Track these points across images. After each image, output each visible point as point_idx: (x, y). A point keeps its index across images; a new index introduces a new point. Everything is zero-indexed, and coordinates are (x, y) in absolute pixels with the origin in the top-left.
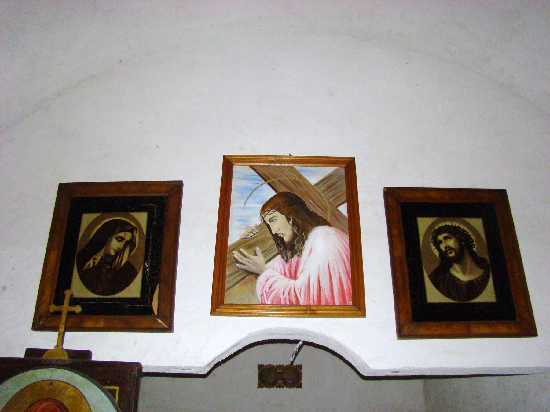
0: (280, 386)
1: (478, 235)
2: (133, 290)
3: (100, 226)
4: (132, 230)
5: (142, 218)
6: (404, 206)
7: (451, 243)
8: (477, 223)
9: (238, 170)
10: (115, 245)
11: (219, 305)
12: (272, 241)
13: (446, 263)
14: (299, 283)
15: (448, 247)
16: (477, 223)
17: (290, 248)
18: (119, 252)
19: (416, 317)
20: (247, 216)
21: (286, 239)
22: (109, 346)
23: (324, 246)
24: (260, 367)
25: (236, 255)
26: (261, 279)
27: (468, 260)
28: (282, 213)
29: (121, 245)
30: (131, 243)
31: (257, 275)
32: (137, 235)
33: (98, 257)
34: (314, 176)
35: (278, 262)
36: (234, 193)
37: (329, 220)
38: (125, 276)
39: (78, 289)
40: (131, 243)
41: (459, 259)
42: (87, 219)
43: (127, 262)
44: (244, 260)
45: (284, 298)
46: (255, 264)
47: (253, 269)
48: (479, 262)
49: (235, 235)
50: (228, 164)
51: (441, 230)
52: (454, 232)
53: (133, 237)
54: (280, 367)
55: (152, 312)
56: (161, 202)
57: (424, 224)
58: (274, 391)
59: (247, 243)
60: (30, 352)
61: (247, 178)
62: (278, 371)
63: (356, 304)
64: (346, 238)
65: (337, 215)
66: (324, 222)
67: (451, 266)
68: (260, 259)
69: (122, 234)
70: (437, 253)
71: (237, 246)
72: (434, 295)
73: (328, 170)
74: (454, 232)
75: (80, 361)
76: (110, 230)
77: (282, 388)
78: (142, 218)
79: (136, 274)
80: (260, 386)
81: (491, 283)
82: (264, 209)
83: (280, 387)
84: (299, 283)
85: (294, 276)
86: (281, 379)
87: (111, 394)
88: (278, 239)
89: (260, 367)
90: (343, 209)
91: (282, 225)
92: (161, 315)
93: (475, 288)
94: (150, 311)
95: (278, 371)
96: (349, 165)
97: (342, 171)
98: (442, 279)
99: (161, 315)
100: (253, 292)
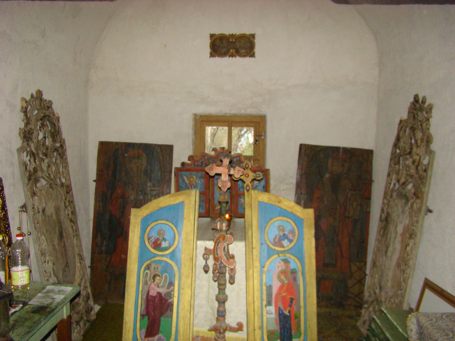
0: (232, 56)
24: (212, 36)
54: (232, 36)
58: (226, 60)
62: (231, 40)
77: (234, 58)
80: (212, 55)
83: (232, 57)
86: (234, 48)
89: (212, 36)
95: (231, 40)
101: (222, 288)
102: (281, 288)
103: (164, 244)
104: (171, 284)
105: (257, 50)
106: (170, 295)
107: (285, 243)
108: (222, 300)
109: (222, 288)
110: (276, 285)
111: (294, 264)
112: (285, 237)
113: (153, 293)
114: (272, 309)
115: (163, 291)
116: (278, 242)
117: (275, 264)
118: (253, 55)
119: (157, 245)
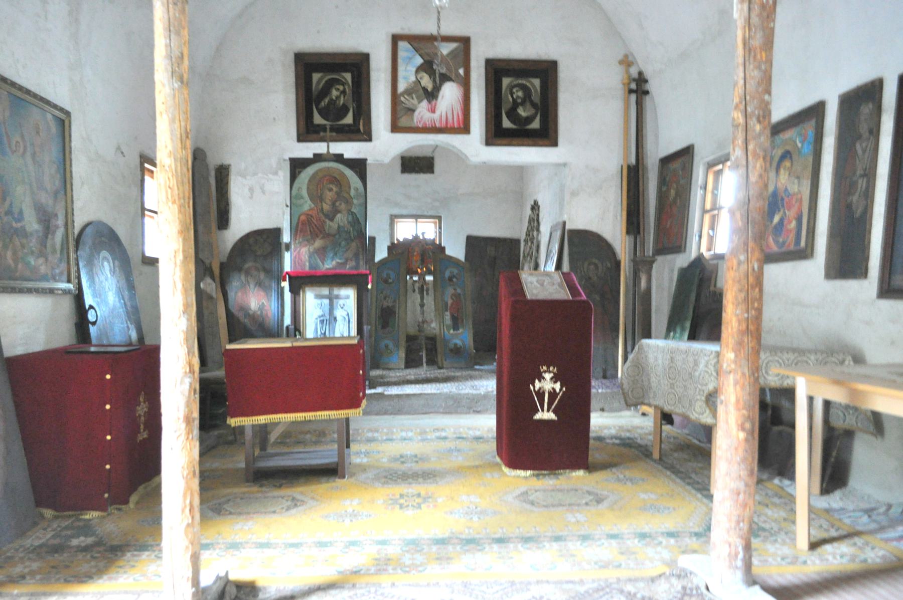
1: (536, 91)
2: (349, 119)
3: (324, 82)
4: (343, 84)
5: (348, 76)
6: (497, 70)
7: (520, 94)
8: (537, 82)
9: (403, 45)
10: (335, 93)
11: (396, 128)
12: (421, 91)
13: (515, 106)
14: (436, 116)
15: (518, 97)
16: (537, 82)
17: (431, 95)
18: (338, 98)
19: (496, 135)
20: (408, 75)
21: (429, 90)
22: (350, 149)
23: (450, 93)
25: (402, 99)
26: (416, 113)
27: (528, 105)
28: (426, 72)
29: (338, 93)
30: (344, 92)
31: (413, 111)
32: (346, 87)
33: (327, 100)
34: (446, 49)
35: (425, 103)
36: (400, 61)
37: (453, 78)
38: (344, 111)
39: (318, 119)
40: (344, 92)
41: (523, 103)
42: (316, 77)
43: (344, 104)
44: (407, 102)
45: (429, 124)
46: (413, 104)
47: (411, 107)
48: (534, 105)
49: (402, 87)
50: (396, 39)
51: (515, 86)
52: (523, 88)
53: (345, 89)
55: (361, 131)
56: (357, 66)
57: (506, 82)
59: (408, 92)
60: (315, 155)
61: (407, 51)
63: (465, 128)
64: (462, 89)
65: (458, 75)
66: (449, 79)
67: (518, 107)
68: (415, 101)
69: (338, 87)
70: (511, 99)
71: (403, 94)
72: (506, 123)
73: (453, 45)
74: (523, 88)
75: (339, 158)
76: (330, 84)
78: (348, 76)
79: (347, 111)
81: (538, 118)
82: (417, 71)
84: (436, 116)
85: (433, 111)
87: (356, 172)
88: (425, 89)
90: (461, 71)
91: (426, 81)
92: (365, 133)
93: (529, 120)
94: (358, 131)
96: (465, 42)
97: (462, 45)
98: (512, 115)
99: (365, 133)
100: (413, 119)
101: (422, 298)
102: (452, 304)
103: (390, 281)
104: (395, 301)
105: (437, 168)
106: (394, 306)
107: (454, 280)
108: (422, 305)
109: (422, 298)
110: (450, 302)
111: (459, 291)
112: (454, 276)
113: (385, 306)
114: (448, 313)
115: (390, 305)
116: (450, 279)
117: (450, 291)
118: (432, 172)
119: (386, 281)
